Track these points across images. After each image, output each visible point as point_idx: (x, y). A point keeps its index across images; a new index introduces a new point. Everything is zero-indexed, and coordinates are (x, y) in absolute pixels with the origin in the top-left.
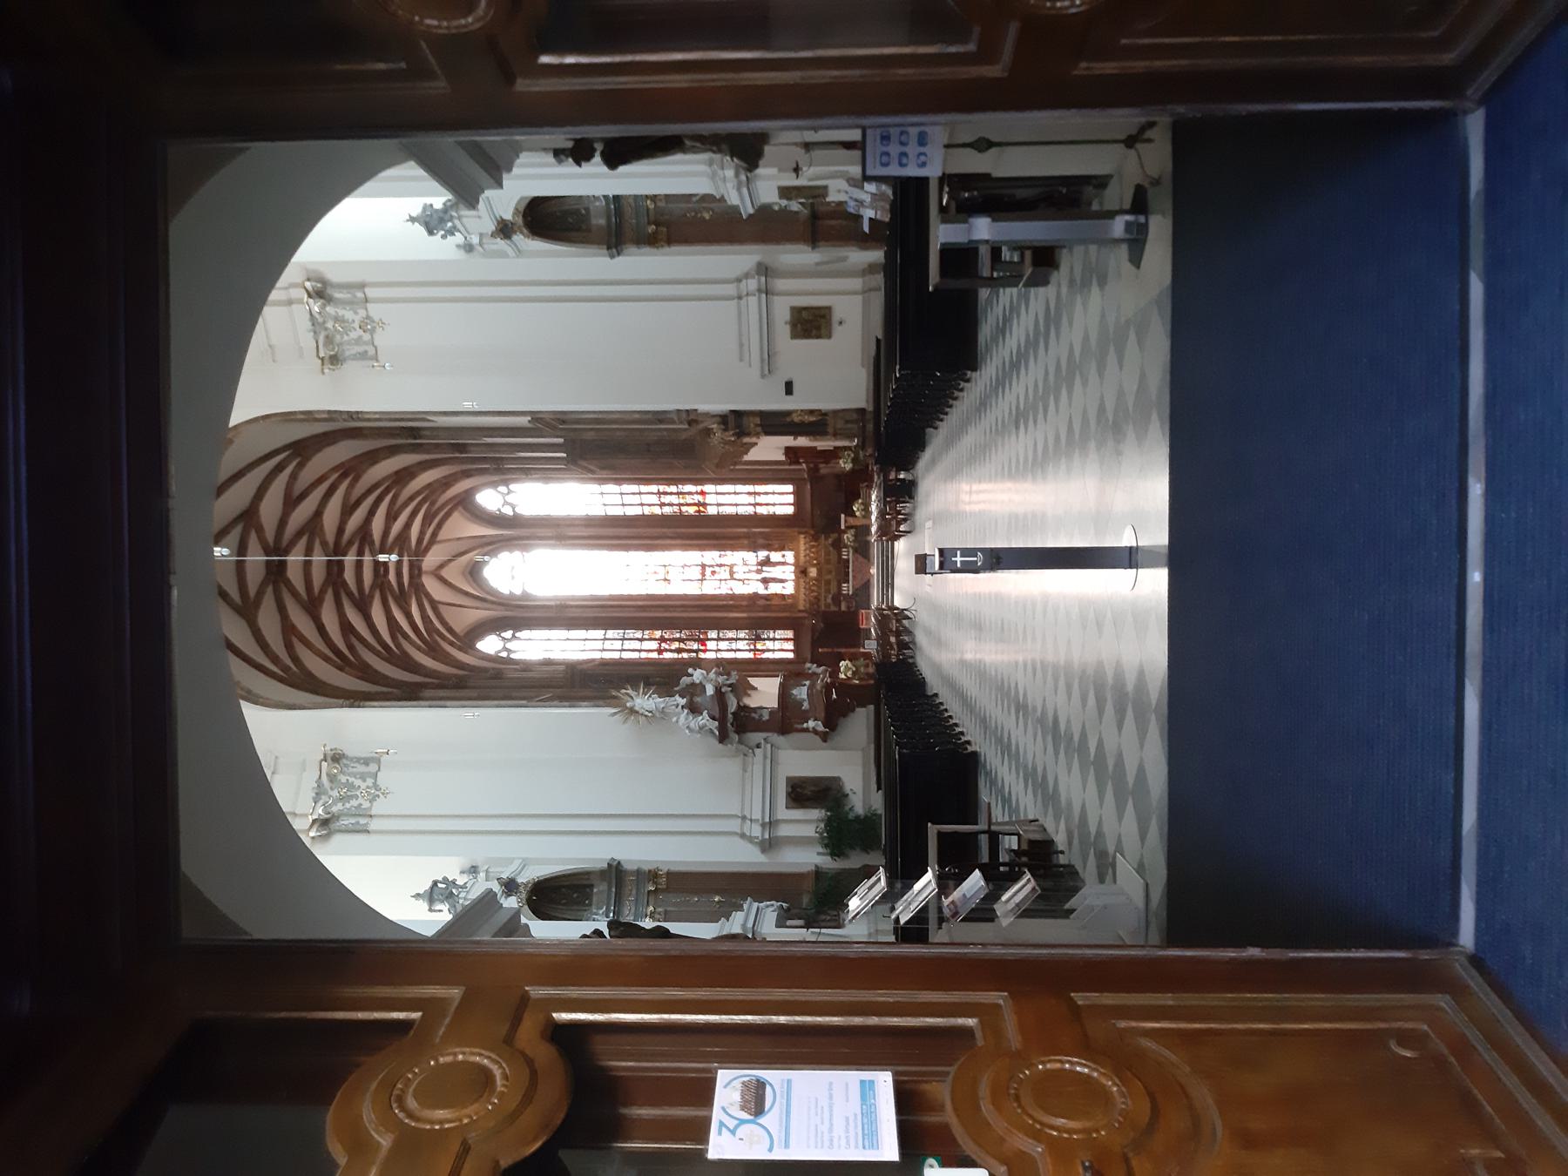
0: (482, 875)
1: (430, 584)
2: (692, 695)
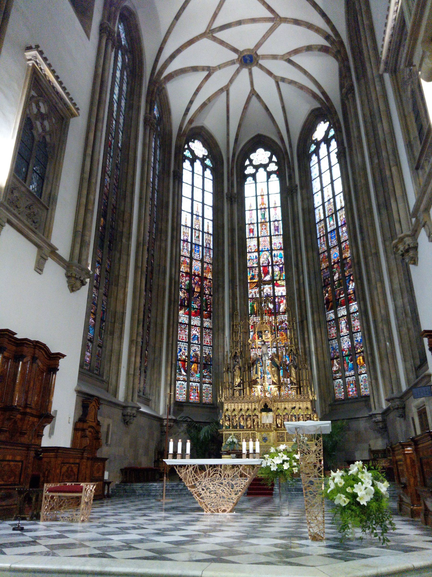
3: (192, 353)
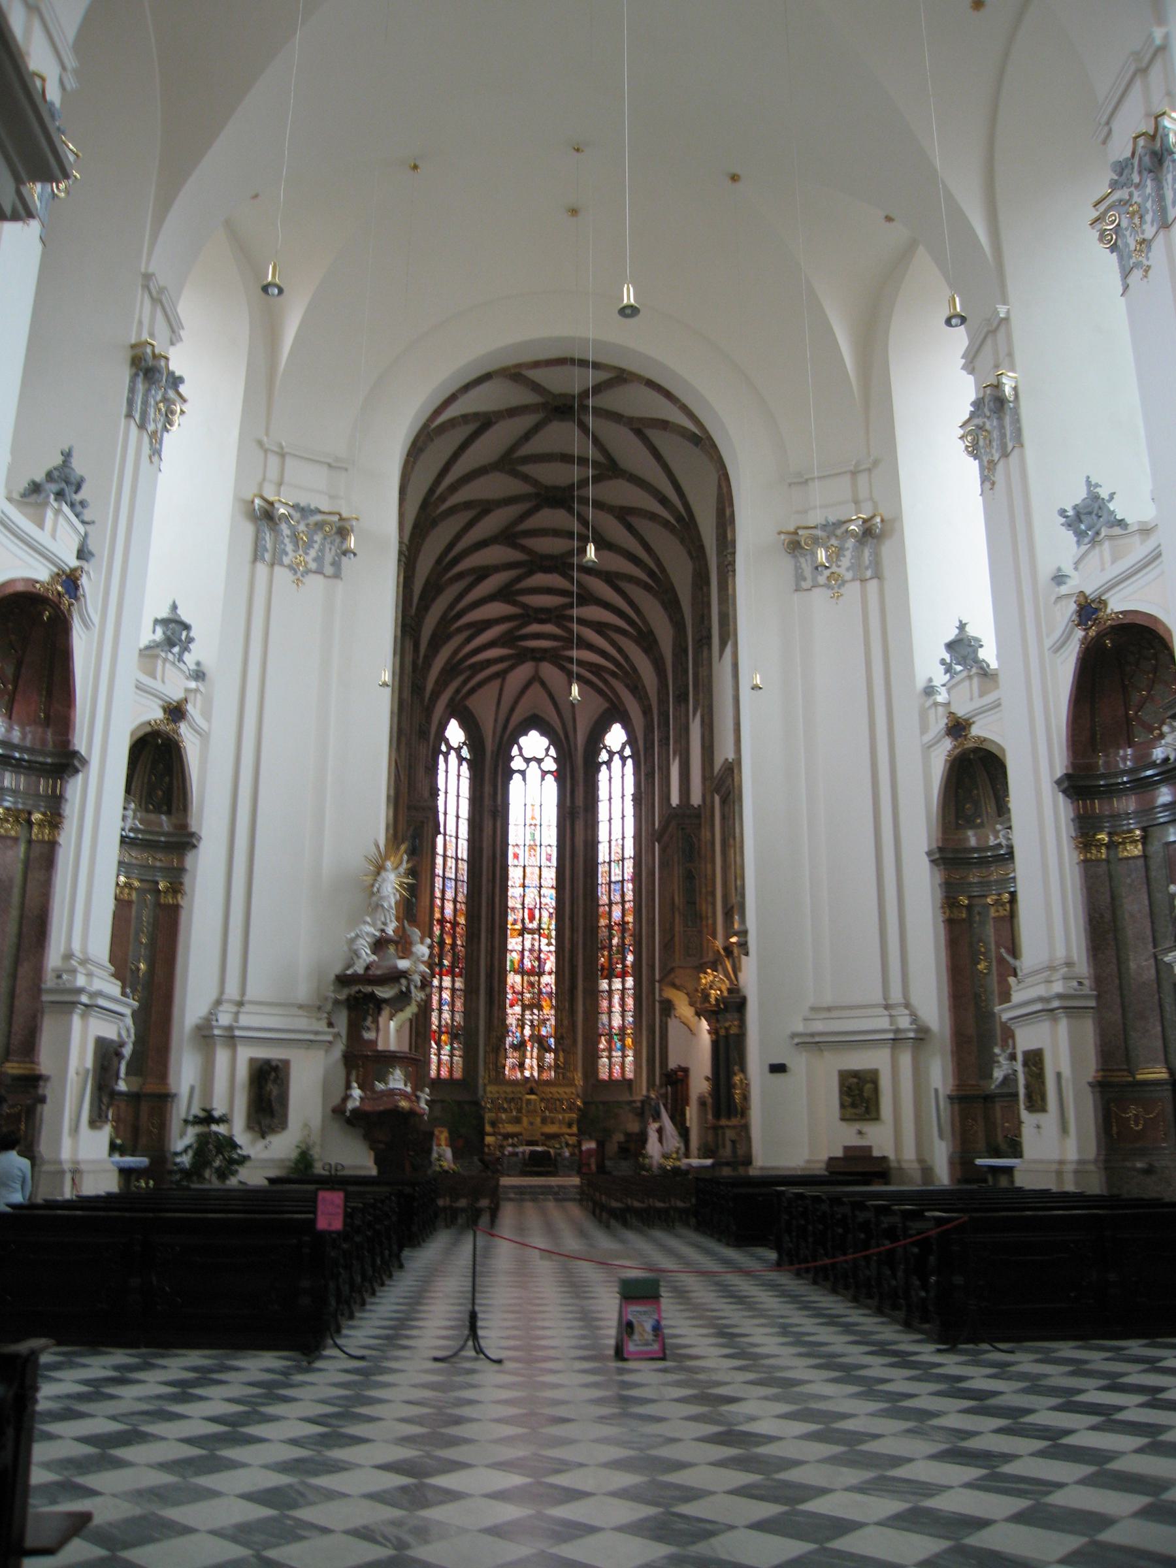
0: (193, 685)
1: (523, 672)
2: (396, 943)
3: (443, 1023)
